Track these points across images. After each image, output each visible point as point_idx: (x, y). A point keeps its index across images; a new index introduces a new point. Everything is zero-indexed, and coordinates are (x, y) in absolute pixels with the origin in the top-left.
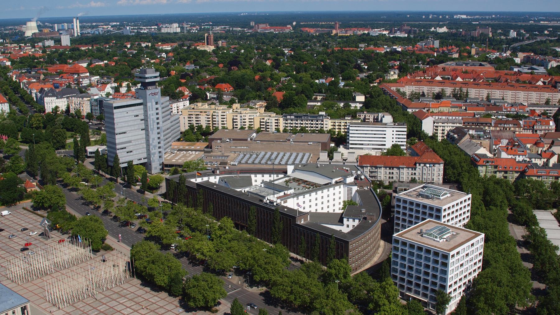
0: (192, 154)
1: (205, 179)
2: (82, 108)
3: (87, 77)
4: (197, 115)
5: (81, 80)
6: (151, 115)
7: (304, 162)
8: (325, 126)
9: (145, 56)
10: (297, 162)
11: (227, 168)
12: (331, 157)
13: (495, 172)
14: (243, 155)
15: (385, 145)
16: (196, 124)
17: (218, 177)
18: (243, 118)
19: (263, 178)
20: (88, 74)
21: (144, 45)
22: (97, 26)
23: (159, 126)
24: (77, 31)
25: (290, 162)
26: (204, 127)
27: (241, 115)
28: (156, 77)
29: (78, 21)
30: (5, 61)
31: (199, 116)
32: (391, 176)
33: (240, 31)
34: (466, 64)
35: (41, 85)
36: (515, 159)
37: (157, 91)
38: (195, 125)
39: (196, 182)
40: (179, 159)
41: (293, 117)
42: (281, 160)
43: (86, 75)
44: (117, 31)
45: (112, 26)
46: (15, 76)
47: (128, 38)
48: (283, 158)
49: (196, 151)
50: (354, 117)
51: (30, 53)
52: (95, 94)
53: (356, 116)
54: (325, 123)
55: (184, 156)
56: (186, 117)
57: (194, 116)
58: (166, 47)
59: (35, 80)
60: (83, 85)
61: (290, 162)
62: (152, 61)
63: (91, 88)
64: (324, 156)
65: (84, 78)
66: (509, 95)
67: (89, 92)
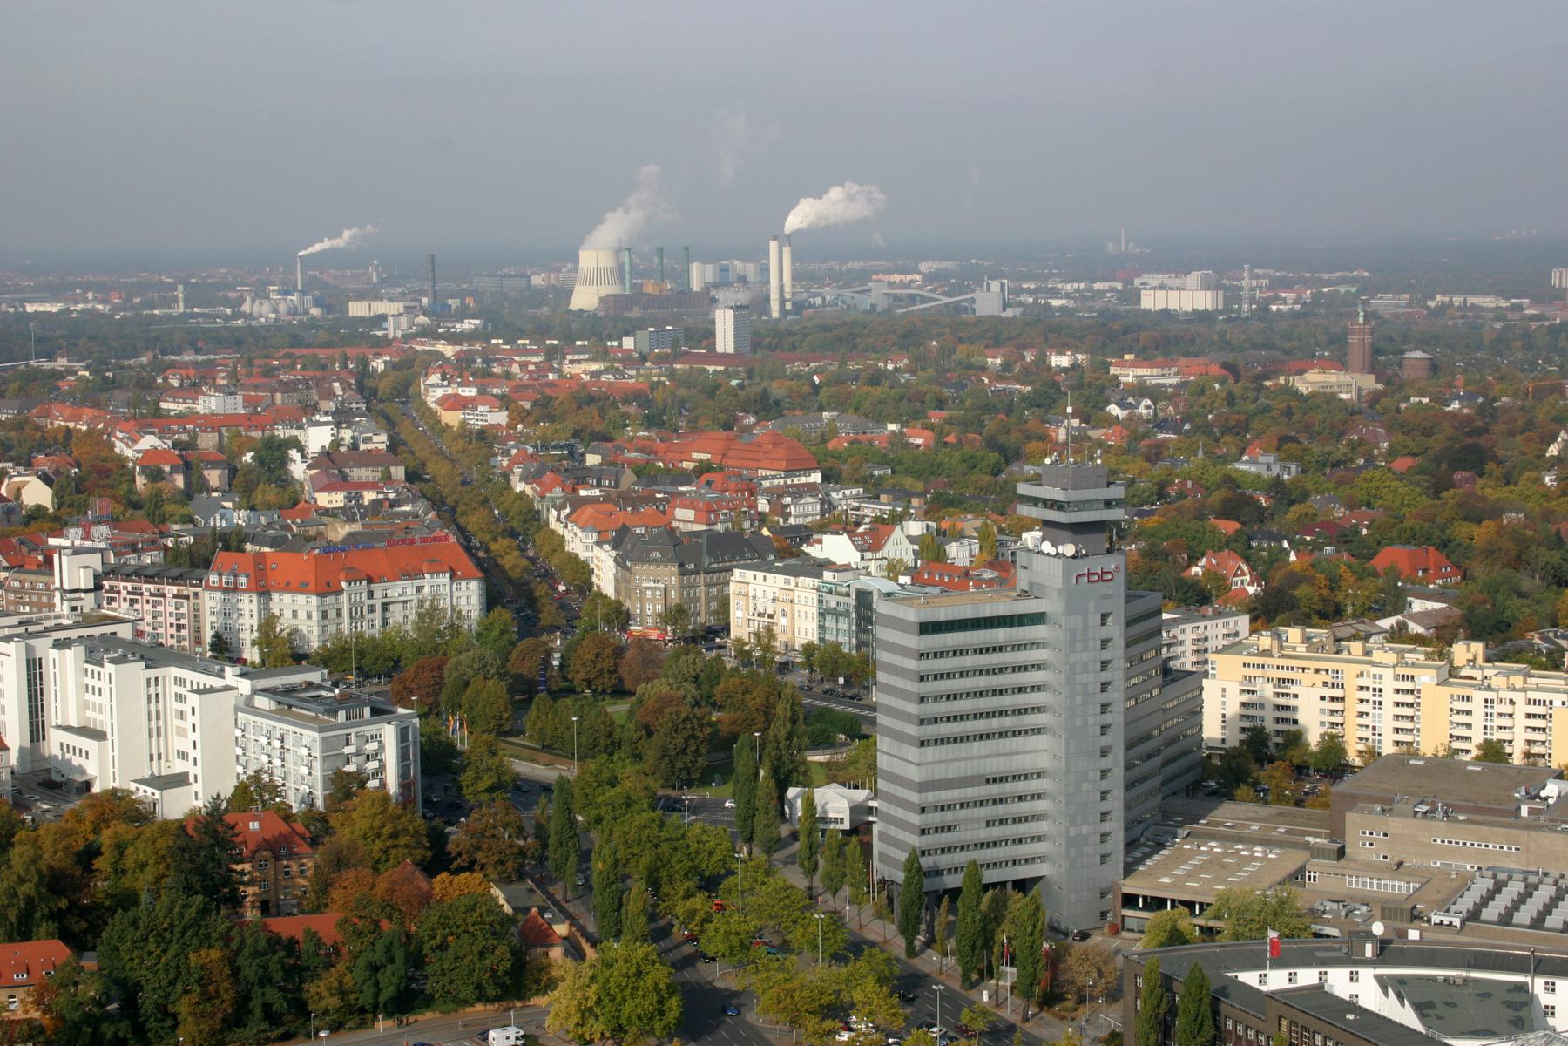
0: (1252, 858)
1: (1307, 977)
2: (783, 621)
3: (811, 489)
5: (788, 500)
6: (1079, 668)
9: (1069, 410)
11: (1413, 935)
14: (1489, 883)
16: (1278, 721)
17: (1367, 974)
18: (1498, 708)
20: (816, 477)
21: (1061, 361)
22: (864, 277)
23: (1108, 719)
24: (781, 288)
26: (1313, 739)
27: (1490, 695)
28: (1108, 504)
29: (787, 251)
31: (1293, 689)
33: (1499, 314)
35: (622, 515)
37: (1113, 563)
39: (1264, 988)
40: (1190, 875)
44: (946, 300)
45: (929, 278)
46: (518, 470)
47: (994, 333)
49: (1268, 843)
51: (586, 378)
52: (840, 560)
55: (1214, 862)
58: (1155, 371)
59: (597, 492)
60: (792, 521)
62: (1095, 434)
63: (827, 538)
65: (799, 492)
67: (814, 551)
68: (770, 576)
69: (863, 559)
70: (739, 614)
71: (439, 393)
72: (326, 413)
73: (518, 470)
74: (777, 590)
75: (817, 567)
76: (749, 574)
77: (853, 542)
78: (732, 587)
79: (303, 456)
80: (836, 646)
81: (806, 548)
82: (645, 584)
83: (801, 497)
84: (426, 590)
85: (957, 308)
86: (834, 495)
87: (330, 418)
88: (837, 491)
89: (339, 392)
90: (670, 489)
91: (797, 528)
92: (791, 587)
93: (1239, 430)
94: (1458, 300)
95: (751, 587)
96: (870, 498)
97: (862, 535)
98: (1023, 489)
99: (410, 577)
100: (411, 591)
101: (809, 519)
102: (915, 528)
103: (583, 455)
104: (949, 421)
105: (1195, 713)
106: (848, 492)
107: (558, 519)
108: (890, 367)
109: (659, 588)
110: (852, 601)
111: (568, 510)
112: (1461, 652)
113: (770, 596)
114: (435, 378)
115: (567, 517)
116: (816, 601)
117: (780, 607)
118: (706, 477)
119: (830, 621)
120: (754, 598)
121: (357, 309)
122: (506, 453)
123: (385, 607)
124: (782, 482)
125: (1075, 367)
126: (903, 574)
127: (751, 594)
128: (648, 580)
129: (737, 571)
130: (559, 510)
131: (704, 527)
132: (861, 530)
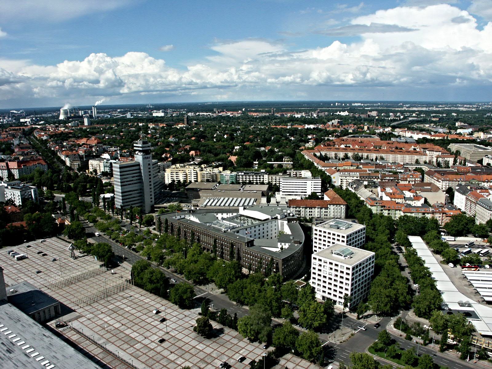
4: (176, 172)
7: (251, 204)
8: (265, 180)
10: (246, 204)
11: (198, 209)
12: (269, 201)
13: (382, 210)
14: (208, 200)
15: (306, 192)
19: (222, 216)
21: (141, 125)
25: (241, 204)
32: (311, 213)
33: (207, 115)
34: (361, 137)
36: (395, 201)
38: (175, 179)
41: (243, 174)
42: (235, 203)
45: (119, 112)
48: (236, 202)
50: (285, 172)
53: (287, 172)
54: (265, 177)
56: (170, 174)
57: (175, 174)
61: (241, 204)
64: (264, 200)
66: (390, 158)
67: (103, 157)
80: (107, 172)
85: (124, 117)
93: (169, 134)
94: (201, 114)
98: (135, 145)
104: (124, 135)
105: (164, 178)
110: (109, 164)
112: (203, 166)
118: (84, 146)
121: (22, 120)
125: (143, 125)
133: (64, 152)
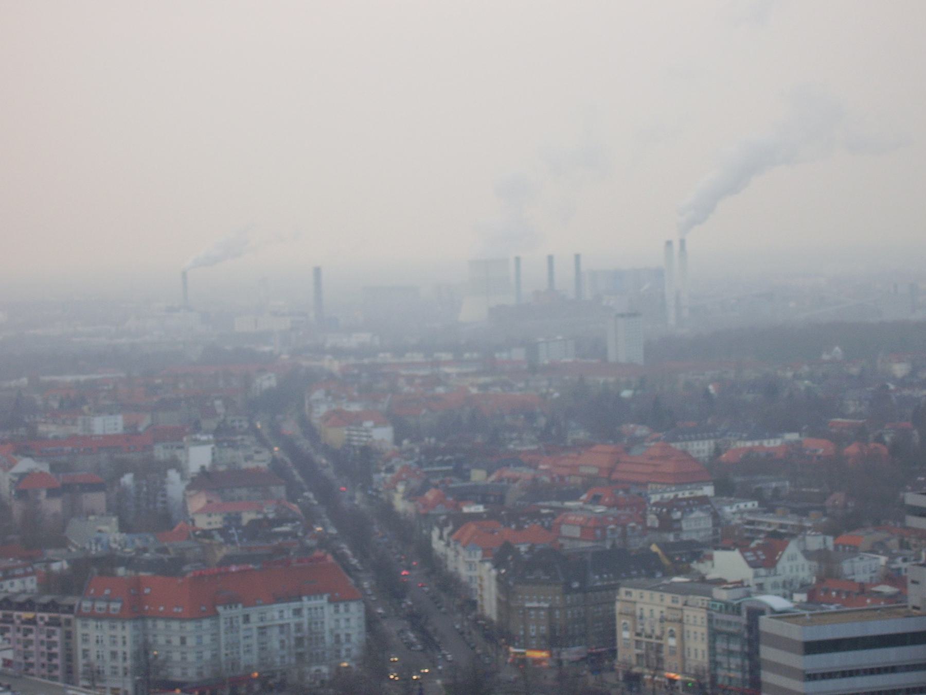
2: (672, 642)
3: (704, 500)
5: (677, 515)
20: (708, 491)
30: (368, 424)
43: (699, 493)
46: (401, 488)
51: (474, 391)
52: (732, 577)
59: (480, 509)
60: (685, 537)
63: (719, 555)
68: (657, 595)
69: (756, 576)
70: (626, 635)
71: (323, 409)
72: (207, 433)
73: (401, 488)
74: (664, 609)
75: (705, 584)
76: (636, 593)
77: (745, 558)
78: (619, 607)
79: (183, 478)
81: (695, 565)
82: (528, 605)
83: (691, 511)
84: (305, 612)
86: (728, 510)
87: (211, 437)
88: (731, 504)
89: (221, 410)
90: (555, 504)
91: (691, 543)
92: (679, 605)
95: (638, 606)
96: (765, 512)
97: (754, 550)
99: (287, 598)
100: (288, 614)
101: (702, 534)
102: (815, 542)
103: (468, 470)
106: (742, 506)
107: (441, 537)
108: (789, 374)
109: (543, 609)
111: (450, 528)
113: (657, 615)
114: (318, 394)
115: (450, 534)
116: (705, 620)
117: (669, 627)
119: (721, 645)
120: (641, 617)
122: (390, 470)
123: (263, 630)
124: (672, 495)
126: (799, 592)
127: (638, 613)
128: (531, 601)
129: (623, 590)
130: (442, 527)
131: (590, 544)
132: (753, 545)
133: (472, 527)
